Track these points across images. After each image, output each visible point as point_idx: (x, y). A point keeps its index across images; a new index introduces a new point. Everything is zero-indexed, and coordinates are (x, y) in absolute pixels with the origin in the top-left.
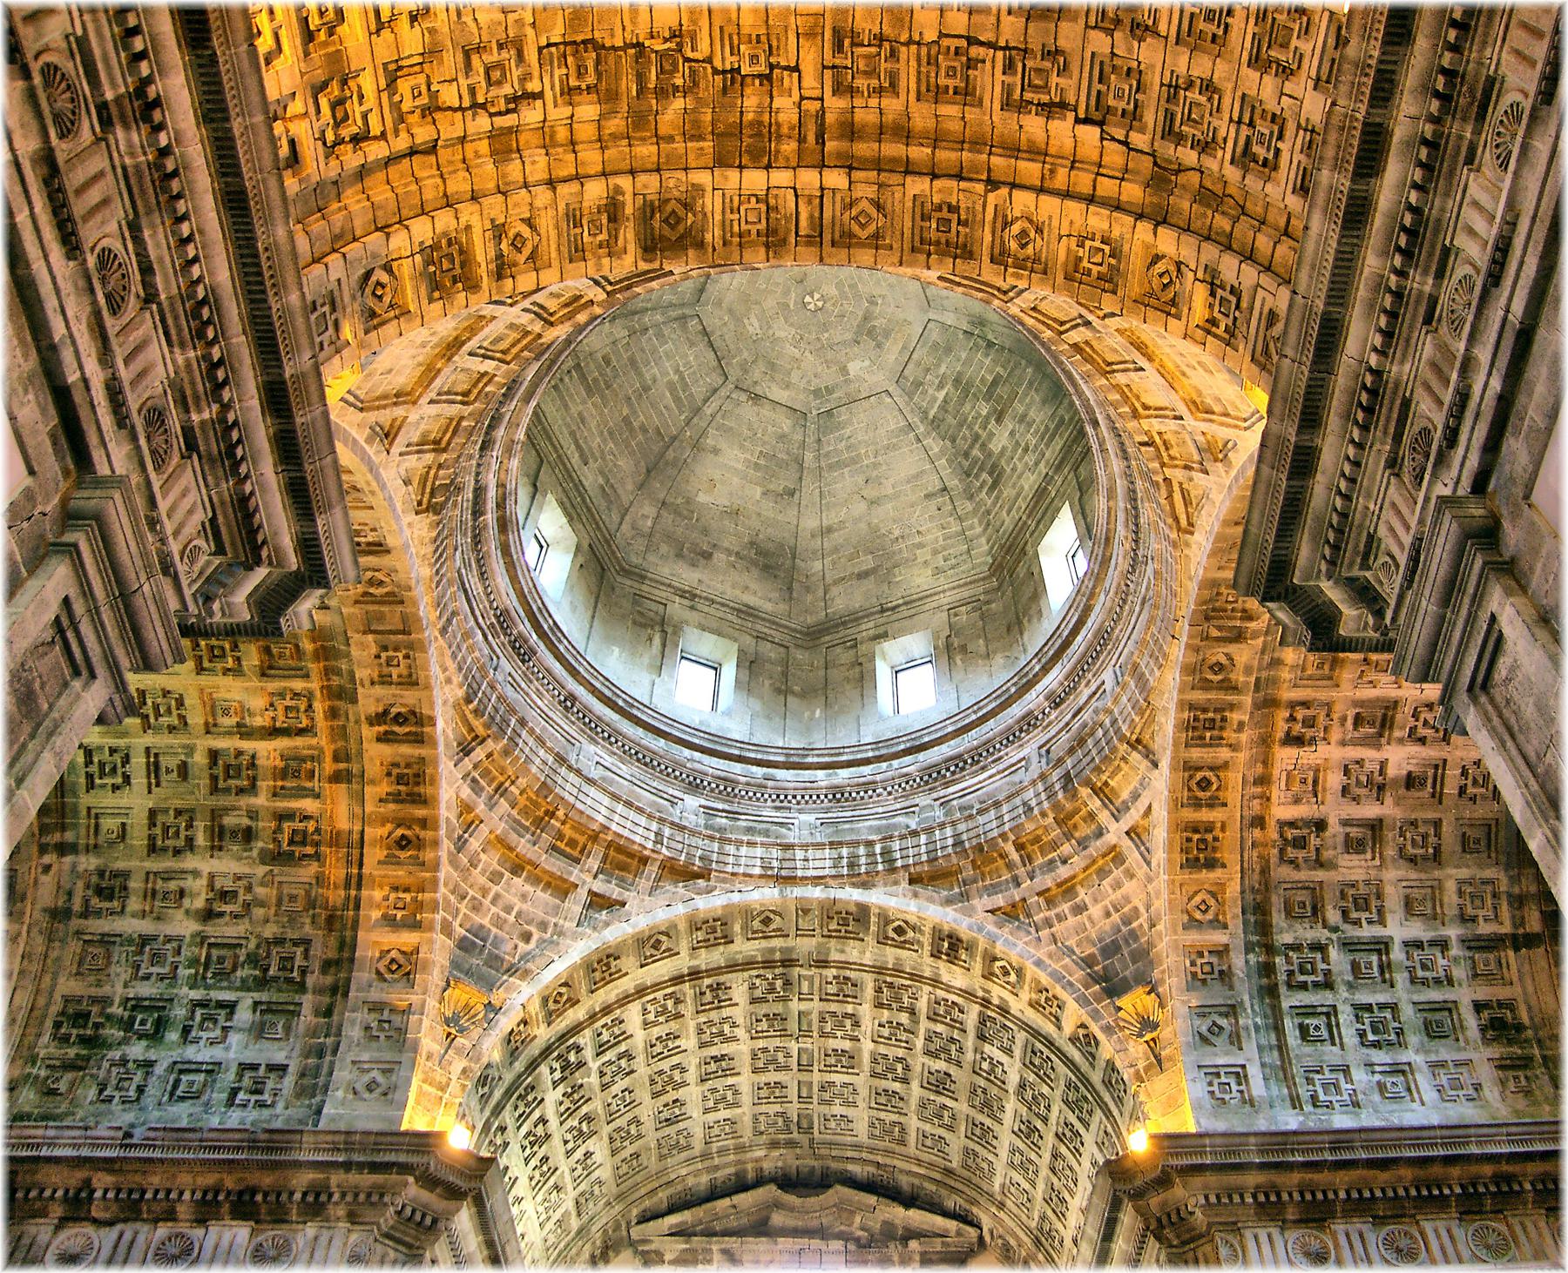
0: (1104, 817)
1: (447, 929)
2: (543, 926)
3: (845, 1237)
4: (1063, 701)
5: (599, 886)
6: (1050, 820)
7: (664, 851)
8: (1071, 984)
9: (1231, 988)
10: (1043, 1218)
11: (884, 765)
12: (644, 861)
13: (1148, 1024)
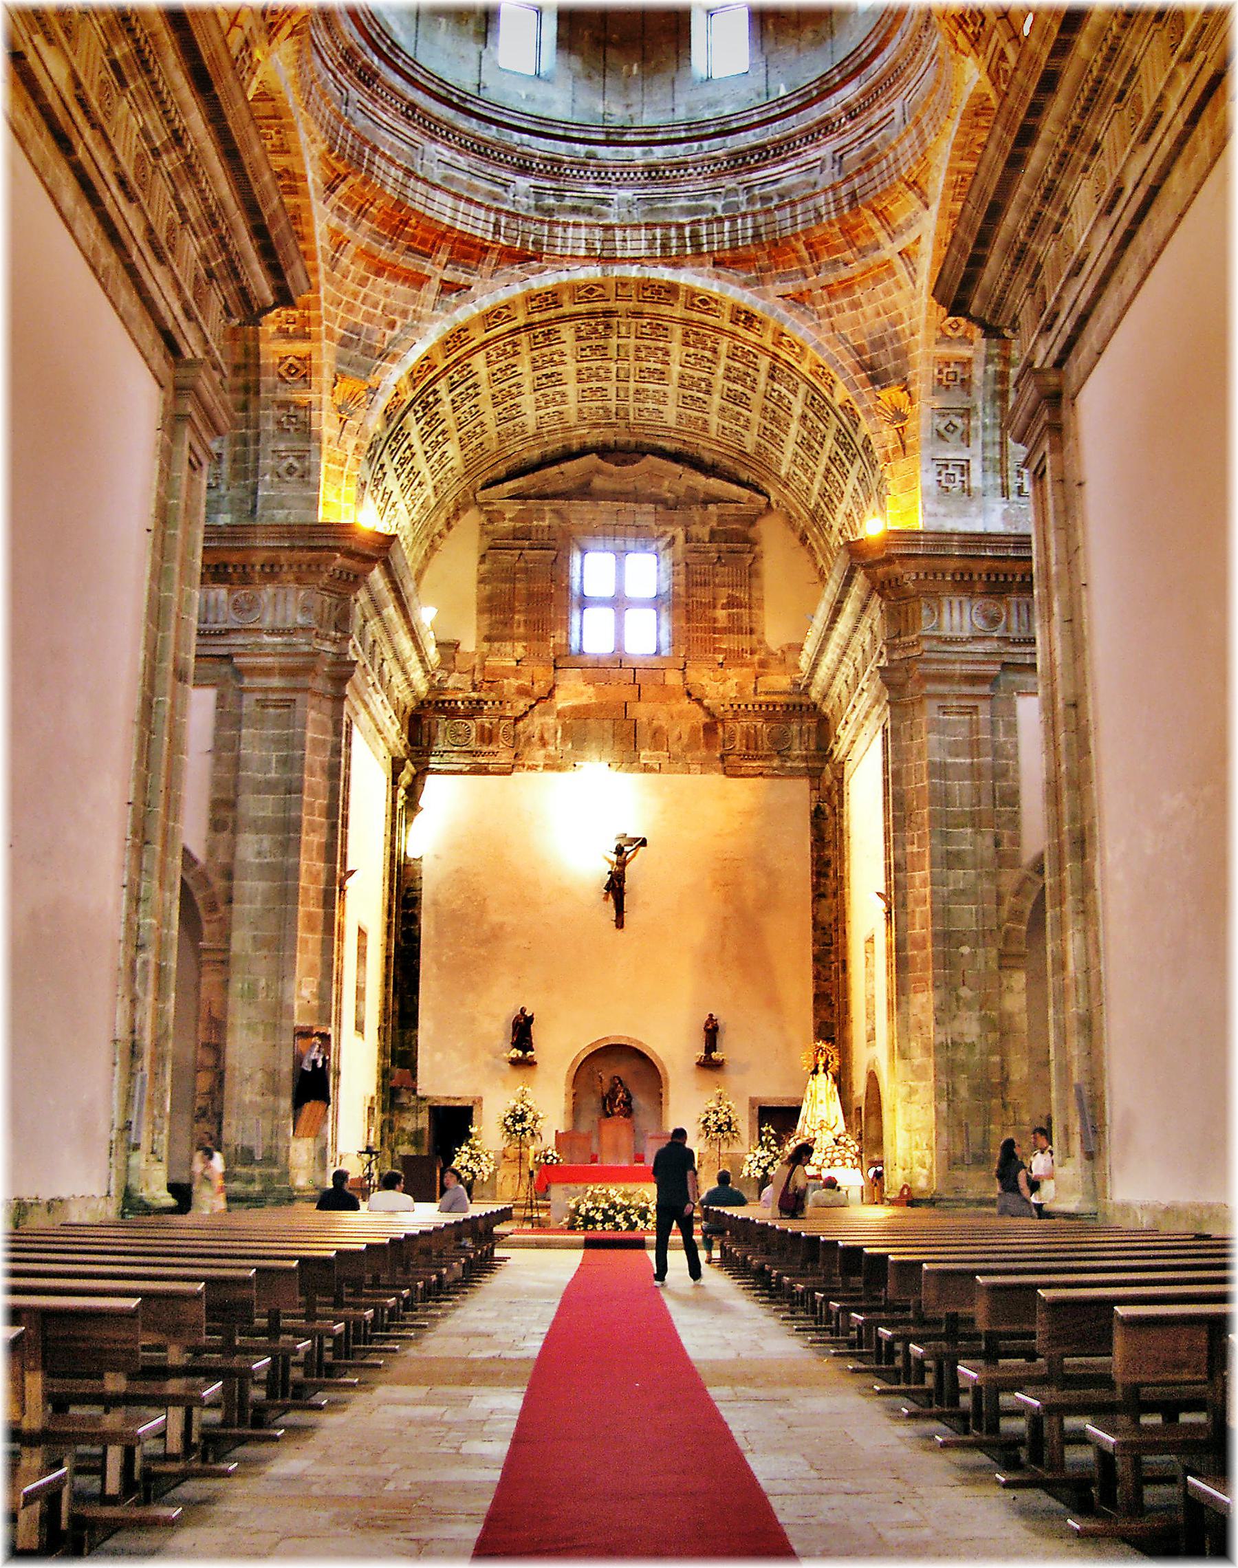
0: (881, 236)
1: (330, 334)
2: (404, 314)
3: (657, 500)
4: (856, 116)
5: (448, 275)
6: (836, 229)
7: (502, 241)
8: (843, 369)
9: (969, 394)
10: (818, 505)
11: (696, 145)
12: (485, 250)
13: (900, 416)
